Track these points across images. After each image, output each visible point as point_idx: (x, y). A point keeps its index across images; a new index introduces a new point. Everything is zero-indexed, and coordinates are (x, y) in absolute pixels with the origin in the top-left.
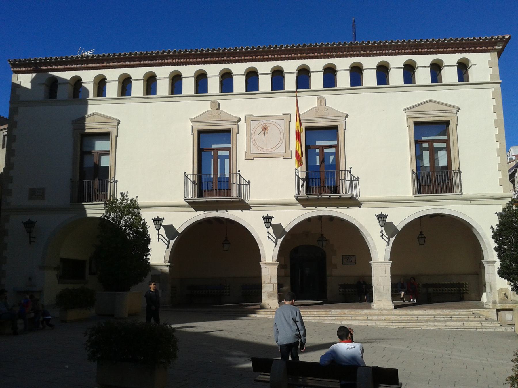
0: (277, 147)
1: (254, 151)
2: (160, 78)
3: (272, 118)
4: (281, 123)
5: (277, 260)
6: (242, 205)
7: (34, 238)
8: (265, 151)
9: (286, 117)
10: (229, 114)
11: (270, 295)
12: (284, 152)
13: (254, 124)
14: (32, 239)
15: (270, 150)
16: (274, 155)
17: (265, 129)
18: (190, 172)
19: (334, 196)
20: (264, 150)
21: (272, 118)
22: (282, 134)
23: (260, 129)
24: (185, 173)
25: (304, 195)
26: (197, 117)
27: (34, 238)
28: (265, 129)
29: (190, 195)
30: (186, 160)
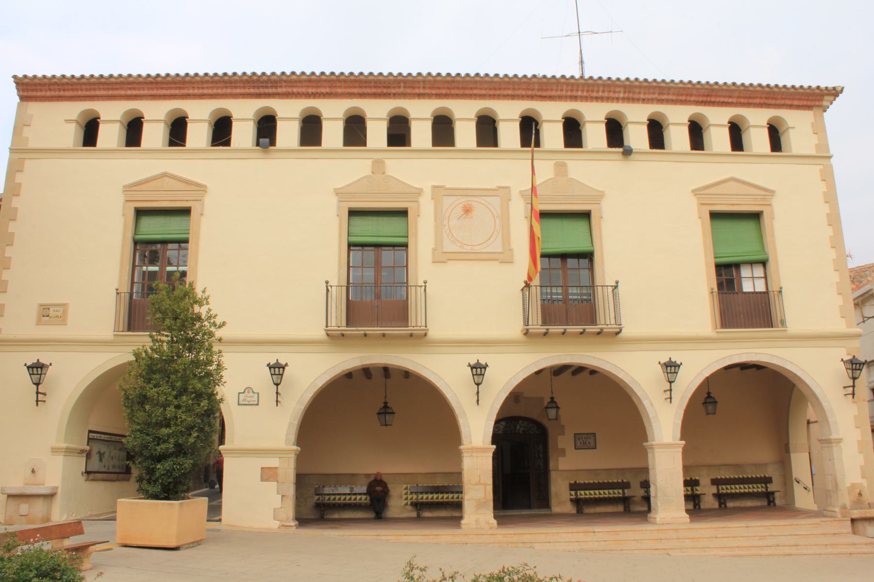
0: (489, 242)
1: (449, 247)
2: (763, 127)
3: (477, 193)
4: (495, 202)
5: (681, 439)
6: (419, 339)
7: (44, 394)
8: (467, 249)
9: (503, 192)
10: (400, 181)
11: (480, 505)
12: (500, 250)
13: (448, 201)
14: (41, 397)
15: (476, 248)
16: (485, 256)
17: (467, 210)
18: (334, 282)
19: (590, 329)
20: (466, 247)
21: (477, 193)
22: (498, 221)
23: (459, 211)
24: (327, 282)
25: (536, 326)
26: (347, 186)
27: (44, 394)
28: (467, 210)
29: (333, 323)
30: (324, 261)
